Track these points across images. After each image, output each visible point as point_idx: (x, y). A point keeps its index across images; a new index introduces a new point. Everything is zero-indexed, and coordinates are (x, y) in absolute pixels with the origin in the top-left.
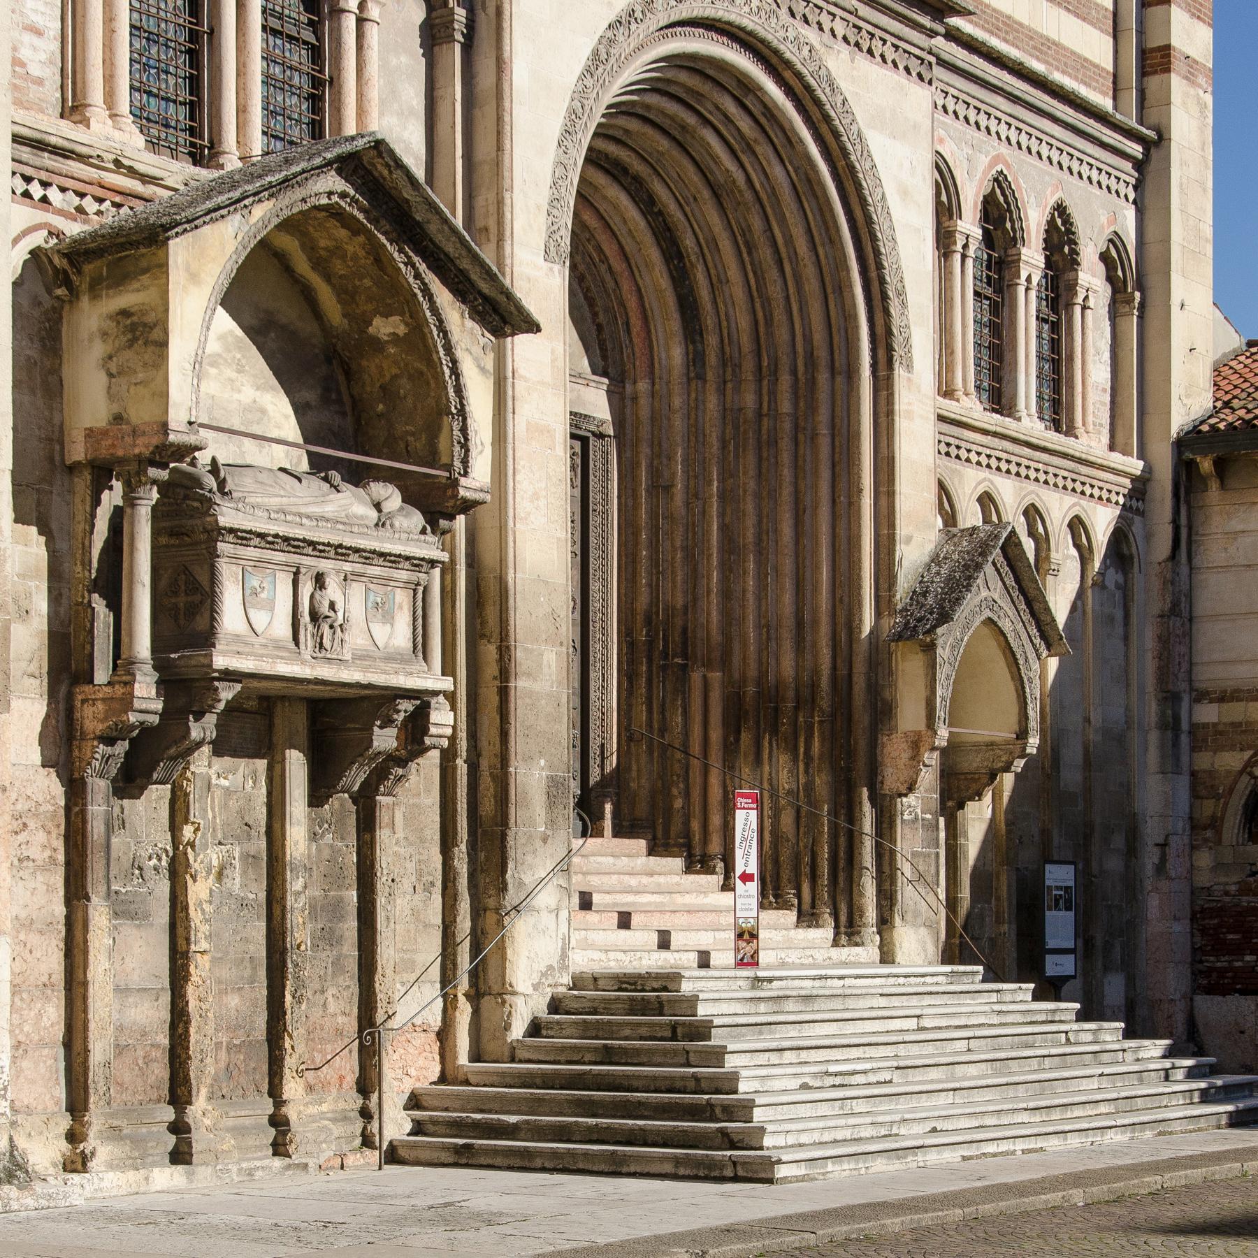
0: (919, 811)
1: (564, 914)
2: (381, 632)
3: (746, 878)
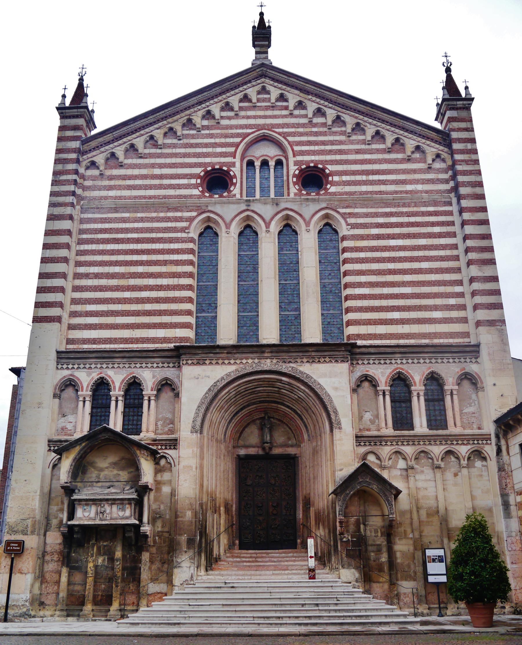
0: (350, 538)
1: (192, 568)
2: (121, 514)
3: (311, 557)
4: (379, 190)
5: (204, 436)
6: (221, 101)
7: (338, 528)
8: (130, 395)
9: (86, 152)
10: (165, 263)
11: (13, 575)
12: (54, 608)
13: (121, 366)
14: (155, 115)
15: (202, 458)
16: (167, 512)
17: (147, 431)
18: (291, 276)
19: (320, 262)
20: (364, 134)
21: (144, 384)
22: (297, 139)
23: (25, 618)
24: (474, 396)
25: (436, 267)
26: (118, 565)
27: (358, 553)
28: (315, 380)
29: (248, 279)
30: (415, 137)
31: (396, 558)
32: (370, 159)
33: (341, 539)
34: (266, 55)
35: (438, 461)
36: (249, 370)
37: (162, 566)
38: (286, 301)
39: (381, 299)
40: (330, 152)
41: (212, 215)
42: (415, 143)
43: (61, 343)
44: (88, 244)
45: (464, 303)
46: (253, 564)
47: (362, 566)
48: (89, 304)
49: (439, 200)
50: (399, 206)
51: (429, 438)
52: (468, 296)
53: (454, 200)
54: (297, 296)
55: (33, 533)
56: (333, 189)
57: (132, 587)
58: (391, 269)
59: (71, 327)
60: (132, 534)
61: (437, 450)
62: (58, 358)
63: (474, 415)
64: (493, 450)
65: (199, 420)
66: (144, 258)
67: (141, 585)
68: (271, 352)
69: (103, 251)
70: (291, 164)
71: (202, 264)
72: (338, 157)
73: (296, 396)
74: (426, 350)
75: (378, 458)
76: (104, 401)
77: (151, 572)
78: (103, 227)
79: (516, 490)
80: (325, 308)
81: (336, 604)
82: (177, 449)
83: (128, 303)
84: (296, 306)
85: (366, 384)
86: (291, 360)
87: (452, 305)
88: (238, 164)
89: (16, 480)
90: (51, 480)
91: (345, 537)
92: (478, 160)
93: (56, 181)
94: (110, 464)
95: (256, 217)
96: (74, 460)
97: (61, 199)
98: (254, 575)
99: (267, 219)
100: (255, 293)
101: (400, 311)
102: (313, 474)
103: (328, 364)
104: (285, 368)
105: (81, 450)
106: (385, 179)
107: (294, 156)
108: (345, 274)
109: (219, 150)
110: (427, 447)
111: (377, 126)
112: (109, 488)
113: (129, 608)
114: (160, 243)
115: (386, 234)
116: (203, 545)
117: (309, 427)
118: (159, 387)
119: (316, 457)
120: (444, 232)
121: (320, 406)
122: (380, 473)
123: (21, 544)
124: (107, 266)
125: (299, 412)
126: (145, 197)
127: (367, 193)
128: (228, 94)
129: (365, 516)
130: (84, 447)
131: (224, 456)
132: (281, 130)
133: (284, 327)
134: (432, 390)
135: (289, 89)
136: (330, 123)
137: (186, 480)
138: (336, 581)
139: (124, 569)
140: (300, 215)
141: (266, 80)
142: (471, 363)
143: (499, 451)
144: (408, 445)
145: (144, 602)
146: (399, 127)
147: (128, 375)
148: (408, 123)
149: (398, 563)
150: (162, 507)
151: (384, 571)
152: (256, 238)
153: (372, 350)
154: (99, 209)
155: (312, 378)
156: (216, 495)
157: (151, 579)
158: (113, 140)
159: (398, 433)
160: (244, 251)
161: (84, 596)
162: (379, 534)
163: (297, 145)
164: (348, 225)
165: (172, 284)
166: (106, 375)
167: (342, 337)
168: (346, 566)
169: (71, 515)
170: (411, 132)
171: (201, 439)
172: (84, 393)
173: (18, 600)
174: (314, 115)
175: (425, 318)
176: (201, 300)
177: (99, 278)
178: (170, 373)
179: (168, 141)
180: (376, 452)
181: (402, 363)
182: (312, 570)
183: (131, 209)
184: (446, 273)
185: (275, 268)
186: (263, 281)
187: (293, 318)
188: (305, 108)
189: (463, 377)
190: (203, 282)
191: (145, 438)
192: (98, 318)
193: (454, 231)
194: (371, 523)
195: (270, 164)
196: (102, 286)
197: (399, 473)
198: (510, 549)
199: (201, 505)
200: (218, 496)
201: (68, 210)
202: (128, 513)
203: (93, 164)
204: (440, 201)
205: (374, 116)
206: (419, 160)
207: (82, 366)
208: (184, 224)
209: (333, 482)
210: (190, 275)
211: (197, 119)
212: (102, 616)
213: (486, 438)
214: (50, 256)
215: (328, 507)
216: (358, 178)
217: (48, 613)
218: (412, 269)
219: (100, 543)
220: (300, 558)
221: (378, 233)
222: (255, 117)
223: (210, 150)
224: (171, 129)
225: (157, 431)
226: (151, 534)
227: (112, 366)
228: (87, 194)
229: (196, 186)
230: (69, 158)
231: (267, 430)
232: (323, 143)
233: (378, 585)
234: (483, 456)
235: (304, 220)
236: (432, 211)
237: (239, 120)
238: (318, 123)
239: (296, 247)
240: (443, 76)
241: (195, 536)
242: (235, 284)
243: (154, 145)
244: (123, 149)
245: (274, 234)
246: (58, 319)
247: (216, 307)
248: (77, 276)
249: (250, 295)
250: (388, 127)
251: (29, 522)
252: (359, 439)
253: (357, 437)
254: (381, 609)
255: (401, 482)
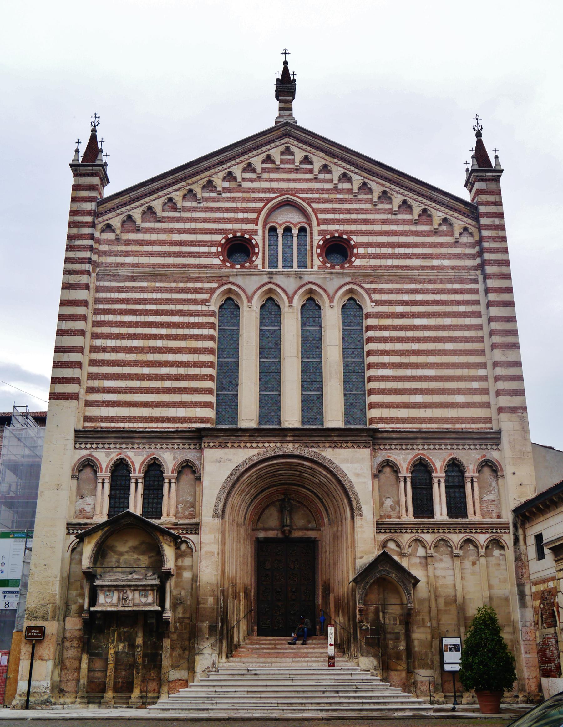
0: (369, 626)
2: (143, 600)
3: (331, 645)
4: (405, 265)
5: (225, 522)
6: (243, 162)
7: (358, 616)
8: (149, 477)
9: (102, 214)
10: (185, 337)
11: (34, 661)
12: (75, 695)
13: (141, 446)
14: (174, 176)
15: (223, 543)
16: (188, 598)
17: (168, 515)
18: (314, 353)
19: (343, 339)
20: (391, 203)
21: (164, 466)
22: (322, 206)
23: (46, 705)
24: (494, 484)
25: (460, 348)
26: (139, 652)
27: (376, 641)
28: (337, 466)
29: (270, 356)
30: (442, 209)
31: (414, 647)
32: (396, 231)
33: (361, 627)
34: (290, 112)
35: (456, 549)
36: (271, 454)
37: (183, 653)
38: (309, 380)
39: (404, 381)
40: (355, 222)
41: (233, 287)
42: (442, 215)
43: (78, 422)
44: (104, 314)
45: (487, 387)
46: (272, 651)
47: (380, 654)
48: (107, 380)
49: (465, 277)
50: (424, 283)
51: (448, 526)
52: (491, 380)
53: (481, 278)
54: (319, 375)
55: (53, 619)
56: (357, 262)
57: (153, 674)
58: (415, 350)
59: (88, 404)
60: (153, 621)
61: (456, 538)
62: (75, 437)
63: (493, 503)
64: (510, 539)
65: (221, 504)
66: (164, 331)
67: (163, 672)
68: (294, 436)
69: (120, 322)
70: (315, 233)
71: (223, 339)
72: (364, 227)
73: (317, 480)
74: (448, 436)
75: (398, 545)
76: (123, 483)
77: (172, 658)
78: (120, 297)
79: (532, 581)
80: (348, 388)
81: (356, 691)
82: (198, 534)
83: (147, 380)
84: (318, 386)
85: (387, 470)
86: (313, 445)
87: (475, 389)
88: (260, 232)
89: (35, 565)
90: (70, 564)
91: (364, 625)
92: (505, 237)
93: (71, 246)
94: (130, 548)
95: (279, 290)
96: (96, 545)
97: (77, 267)
98: (274, 662)
99: (290, 293)
100: (276, 371)
101: (423, 394)
102: (333, 560)
103: (350, 450)
104: (307, 452)
105: (103, 535)
106: (411, 252)
107: (319, 225)
108: (369, 353)
109: (240, 215)
110: (446, 535)
111: (405, 196)
112: (131, 574)
113: (150, 695)
114: (179, 316)
115: (411, 312)
116: (225, 632)
117: (329, 511)
118: (180, 469)
119: (336, 543)
120: (469, 312)
121: (341, 492)
122: (399, 561)
123: (42, 630)
124: (125, 339)
125: (320, 496)
126: (163, 265)
127: (392, 267)
128: (250, 155)
129: (385, 604)
130: (106, 532)
131: (244, 540)
132: (305, 196)
133: (306, 407)
134: (453, 476)
135: (313, 151)
136: (355, 190)
137: (208, 566)
138: (356, 669)
139: (145, 655)
140: (324, 290)
141: (291, 140)
142: (492, 450)
143: (516, 541)
144: (428, 532)
145: (165, 689)
146: (427, 197)
147: (148, 457)
148: (436, 194)
149: (416, 651)
150: (183, 593)
151: (402, 660)
152: (278, 312)
153: (394, 435)
154: (115, 277)
155: (334, 463)
156: (236, 580)
157: (172, 666)
158: (130, 202)
159: (418, 520)
160: (266, 326)
161: (105, 684)
162: (398, 622)
163: (321, 213)
164: (372, 301)
165: (192, 360)
166: (125, 456)
167: (364, 419)
168: (365, 654)
169: (93, 601)
170: (439, 203)
171: (222, 524)
172: (103, 474)
173: (38, 687)
174: (340, 180)
175: (448, 402)
176: (221, 377)
177: (116, 352)
178: (191, 455)
179: (188, 204)
180: (396, 539)
181: (423, 449)
182: (331, 658)
183: (149, 278)
184: (470, 355)
185: (298, 345)
186: (286, 359)
187: (315, 399)
188: (330, 172)
189: (484, 464)
190: (224, 358)
191: (166, 522)
192: (116, 395)
193: (479, 310)
194: (390, 611)
195: (293, 231)
196: (119, 360)
197: (418, 561)
198: (524, 639)
199: (223, 591)
200: (238, 581)
201: (84, 279)
202: (150, 599)
203: (109, 228)
204: (466, 279)
205: (401, 184)
206: (446, 232)
207: (100, 446)
208: (205, 296)
209: (353, 569)
210: (210, 351)
211: (218, 181)
212: (124, 703)
213: (505, 527)
214: (66, 328)
215: (348, 594)
216: (384, 251)
217: (68, 700)
218: (436, 350)
219: (120, 629)
220: (319, 646)
221: (402, 311)
222: (278, 180)
223: (231, 215)
224: (190, 191)
225: (177, 515)
226: (172, 620)
227: (132, 446)
228: (103, 259)
229: (216, 255)
230: (84, 221)
231: (287, 513)
232: (349, 211)
233: (396, 673)
234: (501, 544)
235: (328, 295)
236: (458, 289)
237: (262, 183)
238: (343, 189)
239: (319, 323)
240: (474, 145)
241: (217, 623)
242: (257, 361)
243: (173, 208)
244: (140, 212)
245: (297, 309)
246: (75, 396)
247: (237, 385)
248: (94, 349)
249: (271, 372)
250: (416, 197)
251: (50, 608)
252: (380, 526)
253: (377, 524)
254: (397, 697)
255: (420, 570)
